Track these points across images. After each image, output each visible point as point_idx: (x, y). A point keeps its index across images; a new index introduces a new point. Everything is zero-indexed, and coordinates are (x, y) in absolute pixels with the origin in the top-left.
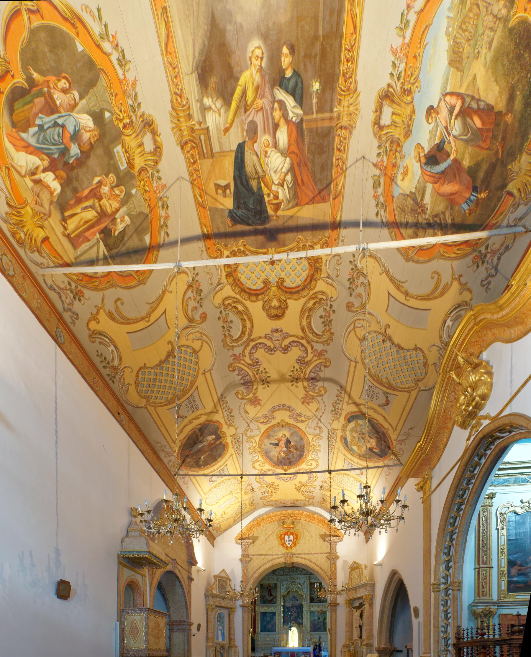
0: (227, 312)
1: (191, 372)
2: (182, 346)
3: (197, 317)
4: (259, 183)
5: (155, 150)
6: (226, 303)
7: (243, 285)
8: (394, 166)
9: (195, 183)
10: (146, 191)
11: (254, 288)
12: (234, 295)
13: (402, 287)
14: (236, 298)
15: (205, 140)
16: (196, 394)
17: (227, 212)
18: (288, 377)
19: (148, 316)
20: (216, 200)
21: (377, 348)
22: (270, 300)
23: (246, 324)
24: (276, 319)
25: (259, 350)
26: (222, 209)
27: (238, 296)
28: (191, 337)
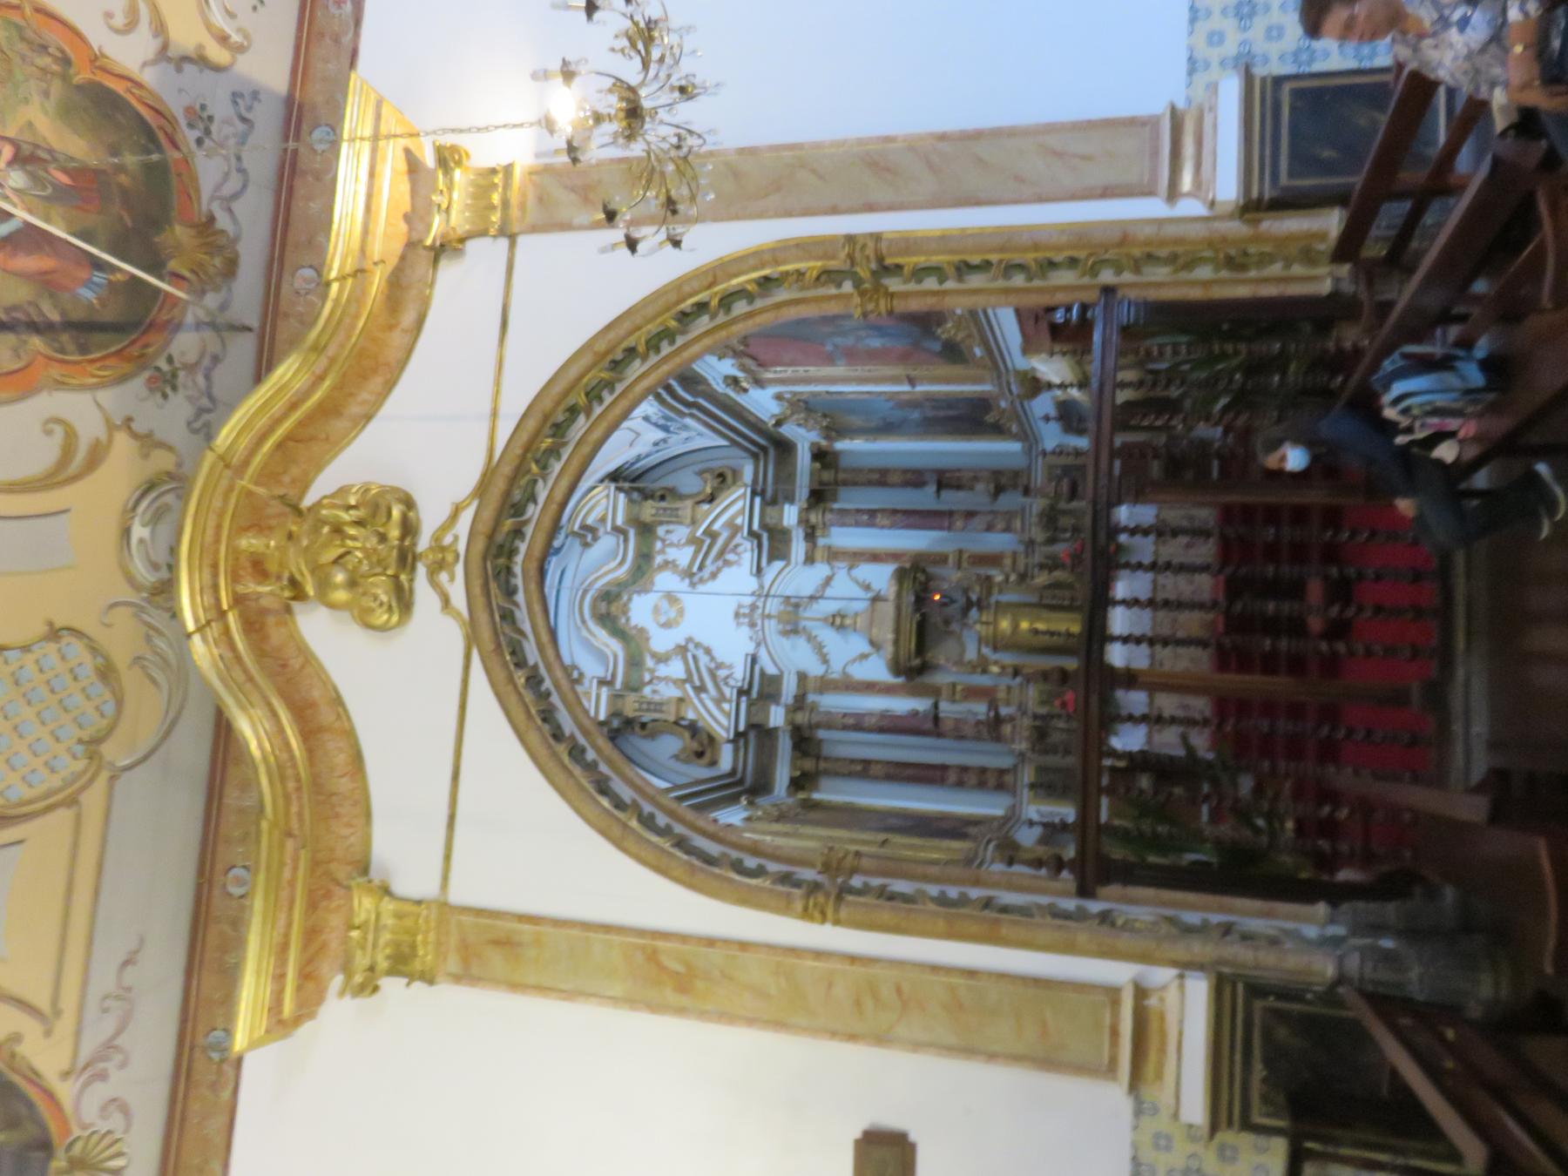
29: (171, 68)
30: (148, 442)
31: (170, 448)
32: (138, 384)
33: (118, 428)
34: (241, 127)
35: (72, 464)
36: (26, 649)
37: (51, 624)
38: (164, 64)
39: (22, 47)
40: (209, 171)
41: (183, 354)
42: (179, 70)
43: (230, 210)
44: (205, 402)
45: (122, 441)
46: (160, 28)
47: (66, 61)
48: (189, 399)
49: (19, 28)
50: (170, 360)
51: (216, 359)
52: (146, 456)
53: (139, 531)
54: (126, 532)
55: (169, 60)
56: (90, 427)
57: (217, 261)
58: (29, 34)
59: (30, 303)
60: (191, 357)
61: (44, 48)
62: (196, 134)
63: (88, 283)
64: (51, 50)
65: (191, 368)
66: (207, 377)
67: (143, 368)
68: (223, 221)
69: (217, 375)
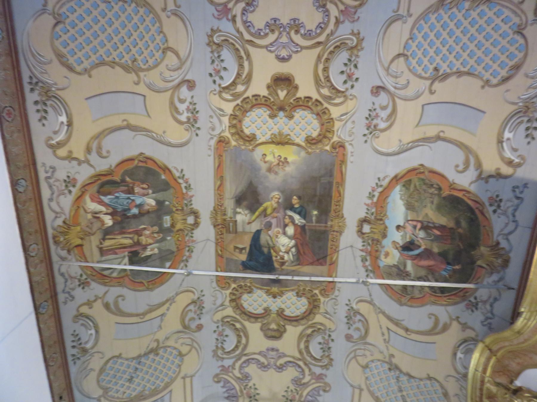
0: (224, 328)
1: (170, 373)
2: (169, 347)
3: (193, 326)
4: (269, 250)
5: (194, 224)
6: (226, 320)
7: (244, 308)
8: (377, 251)
9: (219, 244)
10: (178, 240)
11: (255, 312)
12: (234, 315)
13: (401, 324)
14: (235, 318)
15: (233, 226)
16: (167, 398)
17: (240, 262)
18: (280, 397)
19: (144, 314)
20: (233, 255)
21: (384, 376)
22: (269, 324)
23: (241, 340)
24: (272, 340)
25: (251, 365)
26: (236, 260)
27: (238, 317)
28: (181, 341)
29: (483, 182)
30: (465, 326)
31: (473, 329)
32: (462, 306)
33: (454, 320)
34: (516, 202)
35: (437, 329)
36: (421, 380)
37: (428, 375)
38: (480, 181)
39: (424, 187)
40: (498, 223)
41: (481, 296)
42: (487, 182)
43: (507, 239)
44: (489, 315)
45: (455, 324)
46: (479, 165)
47: (440, 189)
48: (482, 313)
49: (423, 180)
50: (476, 298)
51: (496, 299)
52: (464, 331)
53: (459, 355)
54: (455, 354)
55: (482, 179)
56: (444, 318)
57: (500, 261)
58: (427, 181)
59: (426, 276)
60: (485, 298)
61: (432, 186)
62: (493, 208)
63: (445, 270)
64: (435, 186)
65: (485, 302)
66: (491, 306)
67: (464, 300)
68: (504, 244)
69: (496, 305)
